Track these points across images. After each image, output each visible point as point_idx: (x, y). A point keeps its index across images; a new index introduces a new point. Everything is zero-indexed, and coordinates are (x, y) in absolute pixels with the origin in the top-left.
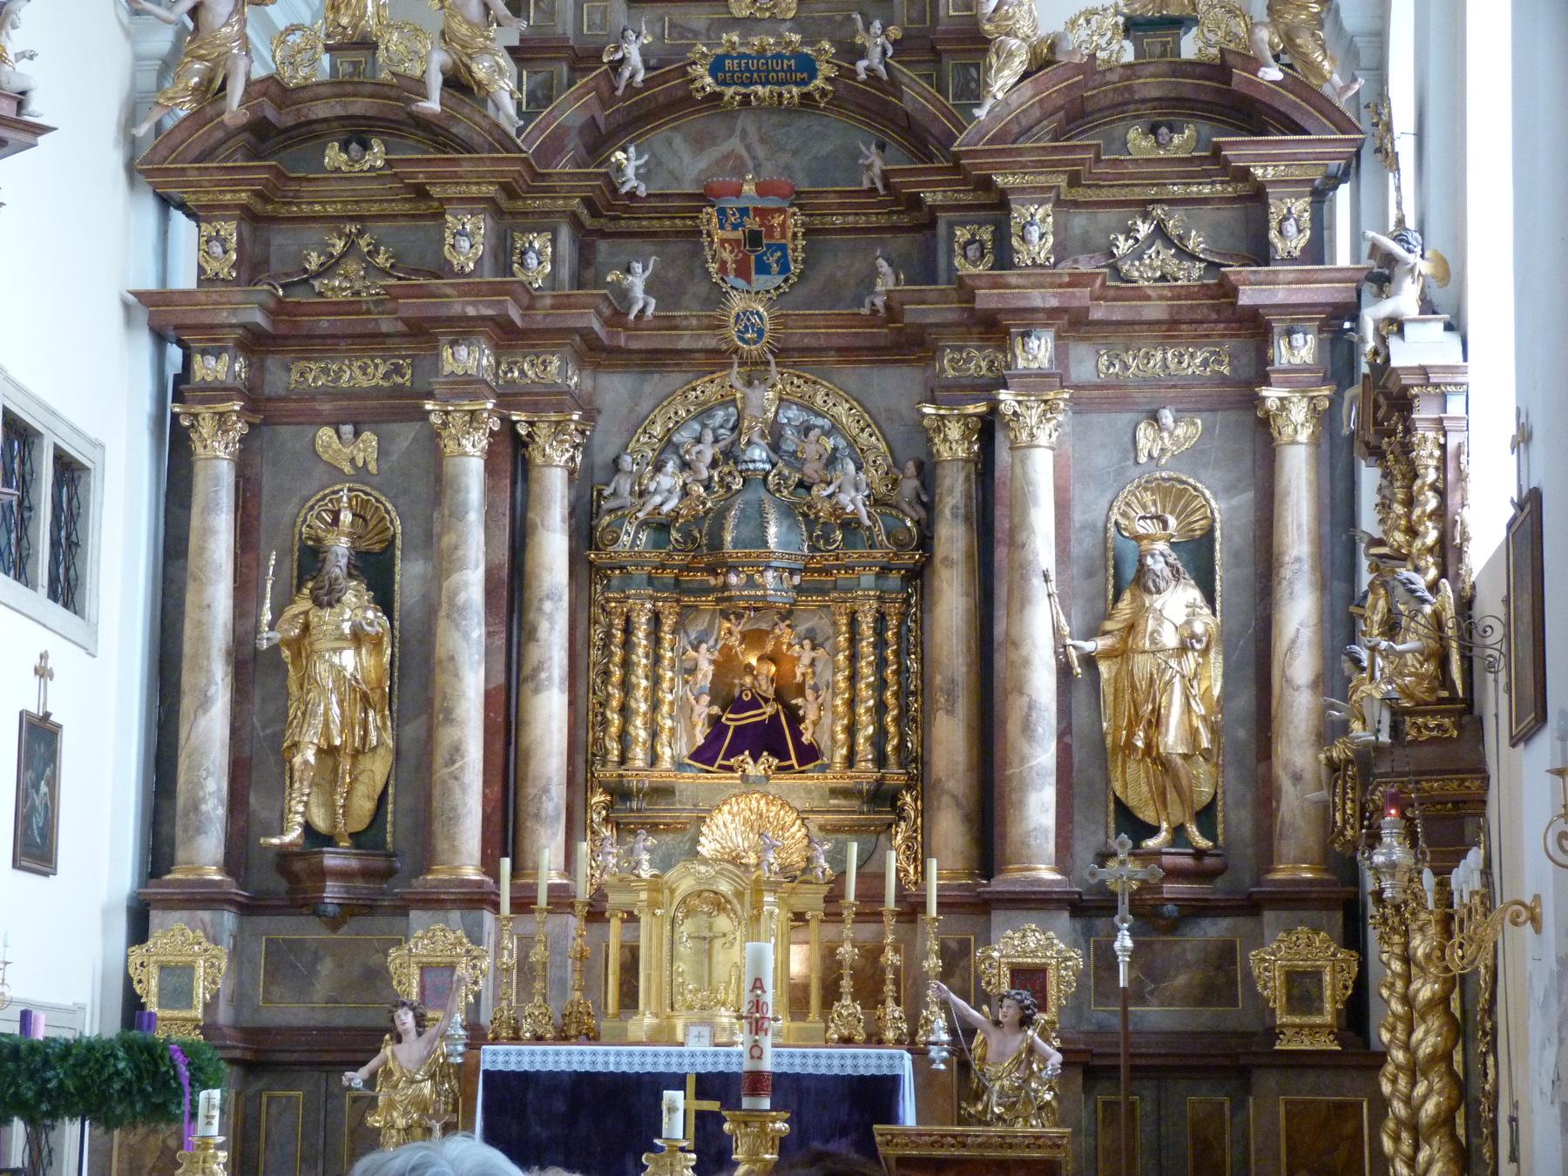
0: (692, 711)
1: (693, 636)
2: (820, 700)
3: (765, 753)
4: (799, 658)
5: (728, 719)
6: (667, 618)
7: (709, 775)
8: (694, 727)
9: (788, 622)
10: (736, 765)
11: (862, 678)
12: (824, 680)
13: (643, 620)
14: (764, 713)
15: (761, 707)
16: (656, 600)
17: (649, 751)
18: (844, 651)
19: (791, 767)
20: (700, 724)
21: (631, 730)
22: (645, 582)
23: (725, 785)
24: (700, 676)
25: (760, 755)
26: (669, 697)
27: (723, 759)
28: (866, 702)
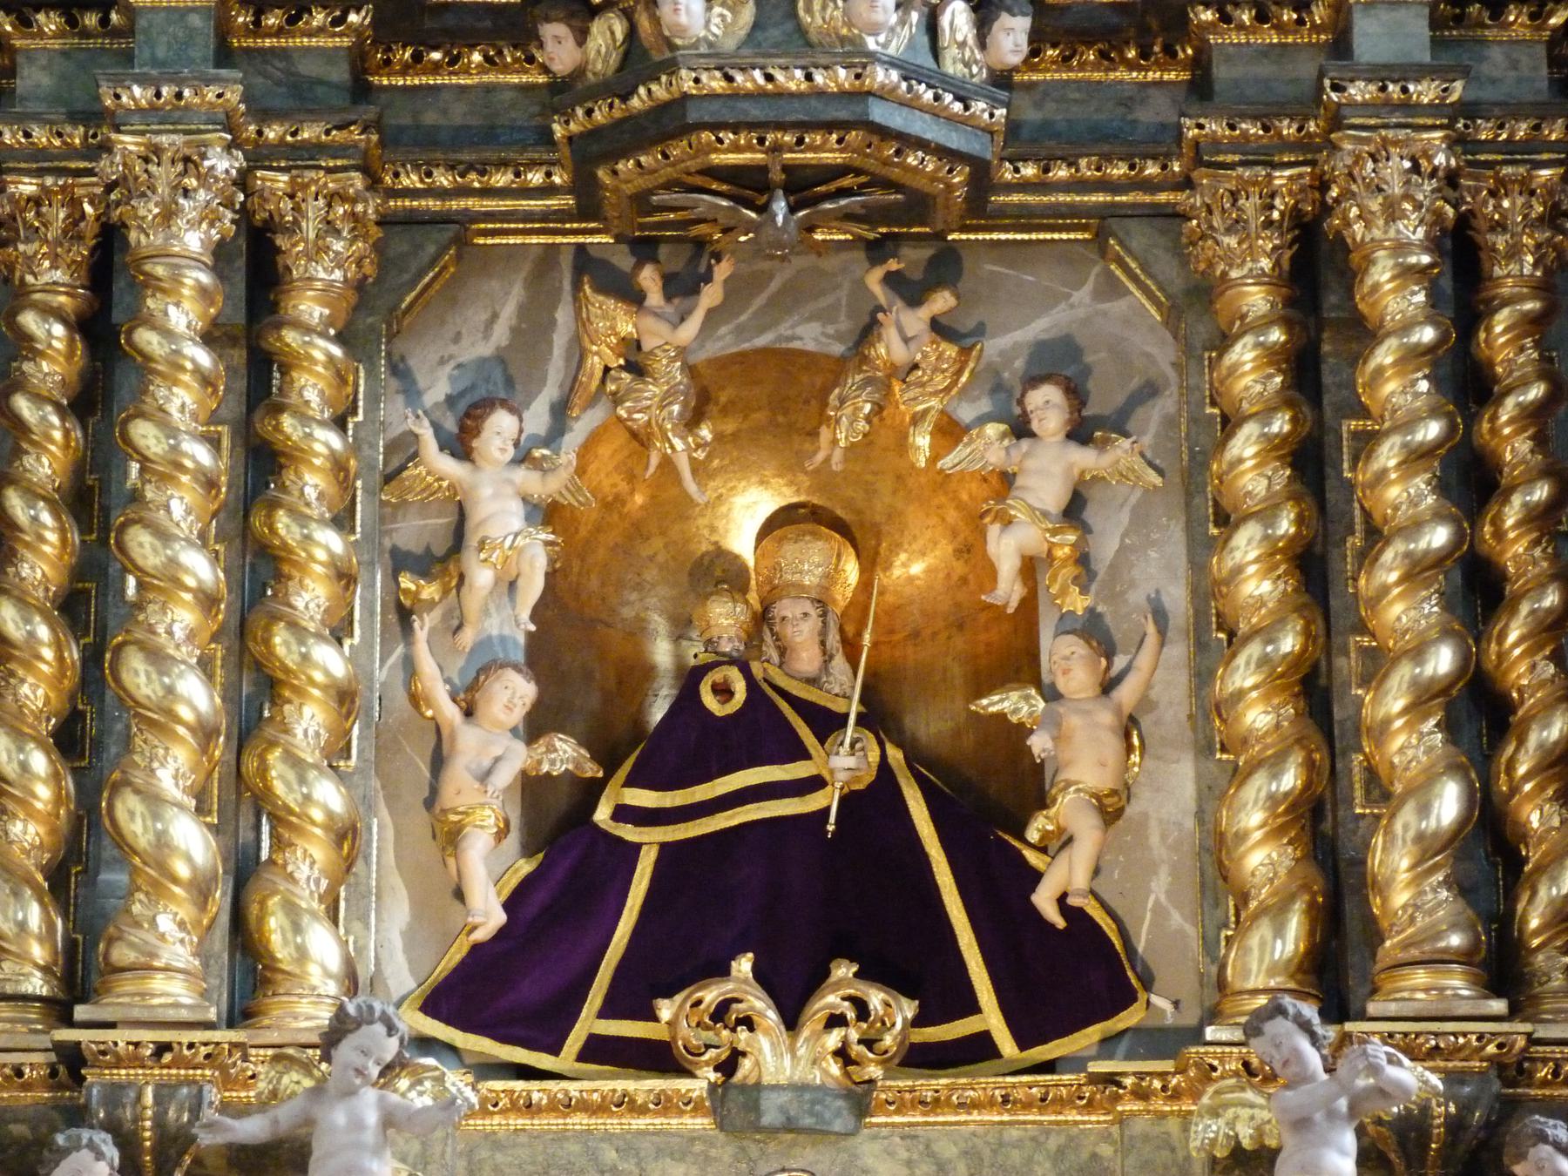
0: (438, 762)
1: (437, 389)
2: (1127, 693)
3: (843, 970)
4: (1006, 480)
5: (623, 813)
6: (318, 251)
7: (537, 1090)
8: (451, 838)
9: (942, 302)
10: (688, 1034)
11: (1376, 536)
12: (1137, 597)
13: (194, 241)
14: (815, 783)
15: (803, 754)
16: (260, 156)
17: (220, 940)
18: (1266, 415)
19: (979, 1049)
20: (488, 819)
21: (131, 815)
22: (205, 46)
23: (627, 1144)
24: (482, 577)
25: (817, 979)
26: (330, 661)
27: (609, 1010)
28: (1418, 652)
